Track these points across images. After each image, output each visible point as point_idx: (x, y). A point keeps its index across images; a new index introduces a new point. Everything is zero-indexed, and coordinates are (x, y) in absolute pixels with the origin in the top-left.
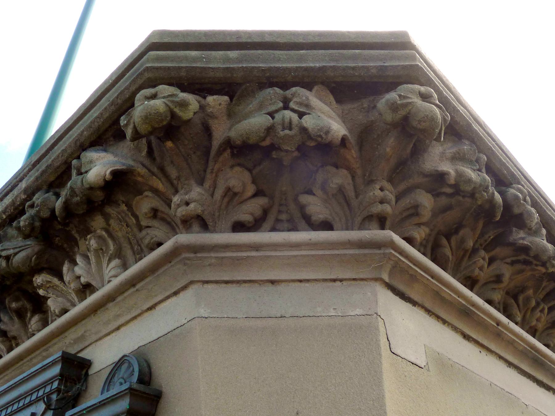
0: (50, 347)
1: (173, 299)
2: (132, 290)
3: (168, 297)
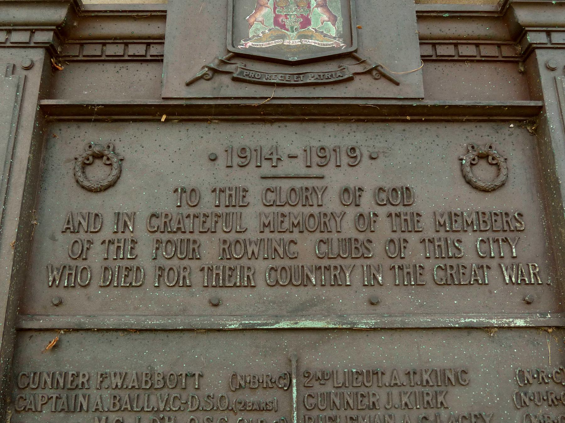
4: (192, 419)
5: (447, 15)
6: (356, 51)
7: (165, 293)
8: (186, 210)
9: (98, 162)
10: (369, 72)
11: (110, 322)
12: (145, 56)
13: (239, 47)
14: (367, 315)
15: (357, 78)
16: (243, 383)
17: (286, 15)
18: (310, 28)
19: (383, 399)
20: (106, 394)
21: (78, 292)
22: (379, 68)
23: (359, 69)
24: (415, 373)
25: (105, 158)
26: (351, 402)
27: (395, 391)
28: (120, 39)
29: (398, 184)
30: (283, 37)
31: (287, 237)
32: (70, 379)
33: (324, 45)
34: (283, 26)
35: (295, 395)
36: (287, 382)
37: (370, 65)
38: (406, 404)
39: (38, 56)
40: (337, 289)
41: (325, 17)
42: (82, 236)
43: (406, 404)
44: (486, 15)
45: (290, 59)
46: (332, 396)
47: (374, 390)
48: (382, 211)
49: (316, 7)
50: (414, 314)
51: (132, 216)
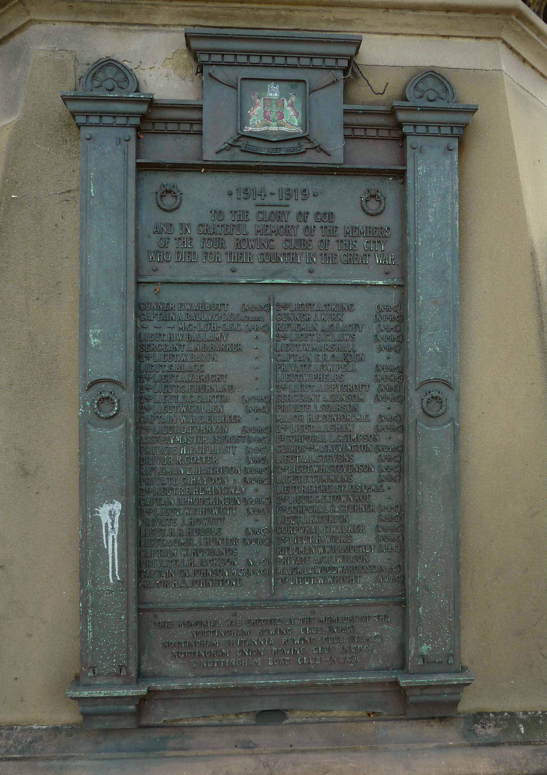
0: (298, 10)
1: (473, 41)
2: (444, 14)
3: (469, 37)
4: (224, 324)
5: (361, 112)
6: (308, 135)
7: (208, 265)
8: (217, 222)
9: (169, 195)
10: (315, 148)
11: (183, 279)
12: (190, 131)
13: (244, 130)
14: (307, 277)
15: (308, 151)
16: (247, 308)
17: (270, 111)
18: (284, 120)
19: (313, 317)
20: (183, 313)
21: (165, 264)
22: (320, 146)
23: (309, 146)
24: (329, 305)
25: (172, 193)
26: (298, 317)
27: (319, 313)
28: (176, 121)
29: (327, 210)
30: (269, 125)
31: (269, 237)
32: (166, 306)
33: (291, 131)
34: (269, 119)
35: (272, 314)
36: (268, 308)
37: (315, 144)
38: (324, 319)
39: (132, 132)
40: (293, 265)
41: (292, 113)
42: (164, 235)
43: (324, 319)
44: (383, 112)
45: (272, 140)
46: (289, 315)
47: (309, 312)
48: (318, 225)
49: (287, 106)
50: (330, 277)
51: (189, 225)
